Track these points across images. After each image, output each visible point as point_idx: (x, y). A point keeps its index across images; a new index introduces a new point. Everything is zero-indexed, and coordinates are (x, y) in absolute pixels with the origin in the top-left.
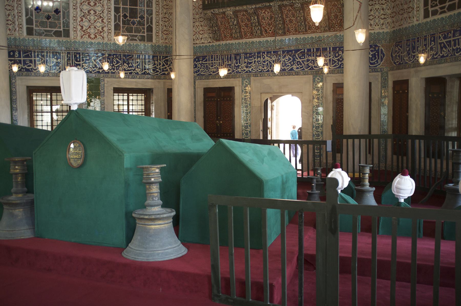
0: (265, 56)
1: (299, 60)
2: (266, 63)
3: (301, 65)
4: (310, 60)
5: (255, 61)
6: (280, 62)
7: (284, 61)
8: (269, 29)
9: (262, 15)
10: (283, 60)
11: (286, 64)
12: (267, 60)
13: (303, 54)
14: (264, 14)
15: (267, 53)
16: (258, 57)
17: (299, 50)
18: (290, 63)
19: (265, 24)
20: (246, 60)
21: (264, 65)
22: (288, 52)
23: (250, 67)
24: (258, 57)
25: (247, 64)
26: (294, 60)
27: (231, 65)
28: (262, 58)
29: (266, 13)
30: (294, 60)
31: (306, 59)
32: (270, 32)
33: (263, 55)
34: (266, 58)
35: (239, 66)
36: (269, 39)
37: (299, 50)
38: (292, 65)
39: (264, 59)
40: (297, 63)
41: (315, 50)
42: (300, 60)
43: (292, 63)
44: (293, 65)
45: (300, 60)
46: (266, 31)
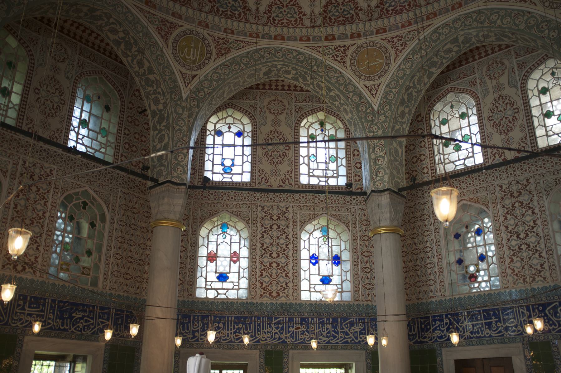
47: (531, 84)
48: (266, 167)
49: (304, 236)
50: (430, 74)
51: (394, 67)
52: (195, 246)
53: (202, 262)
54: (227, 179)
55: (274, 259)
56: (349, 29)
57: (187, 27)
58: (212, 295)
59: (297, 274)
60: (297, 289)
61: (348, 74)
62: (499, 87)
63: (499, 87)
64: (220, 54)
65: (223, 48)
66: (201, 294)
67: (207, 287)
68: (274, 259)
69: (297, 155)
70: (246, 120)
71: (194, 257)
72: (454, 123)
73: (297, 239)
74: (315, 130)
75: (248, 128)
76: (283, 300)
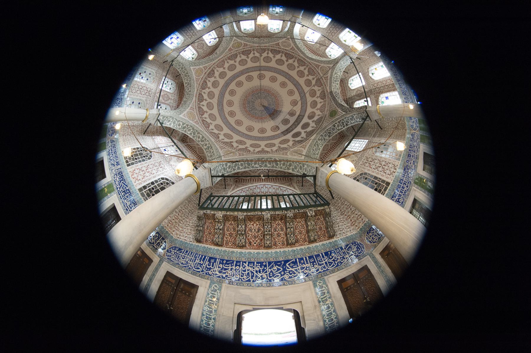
0: (247, 265)
1: (291, 269)
2: (247, 272)
3: (294, 273)
4: (304, 268)
5: (231, 269)
6: (266, 272)
7: (271, 271)
8: (253, 241)
9: (250, 226)
10: (270, 270)
11: (273, 275)
12: (248, 270)
13: (295, 263)
14: (252, 226)
15: (249, 263)
16: (236, 265)
17: (288, 261)
18: (280, 273)
19: (250, 236)
20: (221, 266)
21: (243, 274)
22: (276, 263)
23: (225, 273)
24: (236, 265)
25: (222, 269)
26: (284, 270)
27: (202, 265)
28: (241, 267)
29: (255, 225)
30: (284, 270)
31: (299, 267)
32: (255, 245)
33: (243, 265)
34: (247, 268)
35: (210, 268)
36: (252, 251)
37: (288, 261)
38: (282, 275)
39: (244, 268)
40: (289, 272)
41: (307, 258)
42: (293, 270)
43: (283, 273)
44: (284, 275)
45: (293, 270)
46: (250, 243)
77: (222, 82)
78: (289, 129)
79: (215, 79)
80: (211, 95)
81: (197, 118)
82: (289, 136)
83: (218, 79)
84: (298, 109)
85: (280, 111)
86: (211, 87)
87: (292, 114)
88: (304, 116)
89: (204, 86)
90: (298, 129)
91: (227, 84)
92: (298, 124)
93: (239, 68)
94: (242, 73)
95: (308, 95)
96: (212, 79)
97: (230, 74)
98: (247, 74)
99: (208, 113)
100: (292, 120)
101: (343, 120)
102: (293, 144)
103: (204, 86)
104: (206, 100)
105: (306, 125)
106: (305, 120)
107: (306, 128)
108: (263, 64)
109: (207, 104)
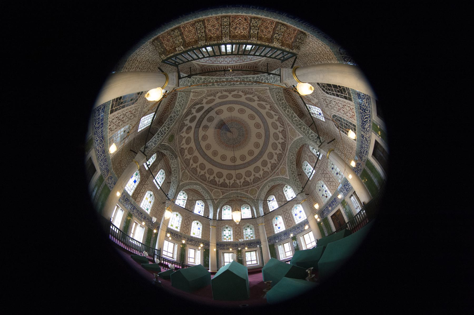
47: (311, 149)
48: (280, 202)
49: (292, 211)
50: (294, 164)
51: (287, 168)
52: (272, 224)
53: (275, 227)
54: (274, 209)
55: (288, 219)
56: (276, 168)
57: (250, 189)
58: (278, 232)
59: (294, 220)
60: (294, 222)
61: (281, 176)
62: (307, 155)
63: (307, 155)
64: (258, 189)
65: (258, 188)
66: (276, 233)
67: (277, 231)
68: (288, 219)
69: (285, 196)
70: (273, 196)
71: (273, 227)
72: (307, 168)
73: (291, 213)
74: (286, 189)
75: (274, 197)
76: (292, 226)
77: (265, 157)
78: (207, 114)
79: (271, 161)
80: (275, 146)
81: (288, 129)
82: (206, 107)
83: (268, 161)
84: (201, 133)
85: (216, 128)
86: (274, 154)
87: (206, 127)
88: (195, 128)
89: (280, 157)
90: (199, 115)
91: (261, 154)
92: (199, 119)
93: (251, 168)
94: (249, 164)
95: (194, 148)
96: (273, 161)
97: (259, 163)
98: (245, 162)
99: (278, 130)
100: (205, 122)
101: (162, 137)
102: (202, 100)
103: (280, 157)
104: (279, 143)
105: (192, 120)
106: (193, 125)
107: (192, 117)
108: (233, 172)
109: (278, 139)
